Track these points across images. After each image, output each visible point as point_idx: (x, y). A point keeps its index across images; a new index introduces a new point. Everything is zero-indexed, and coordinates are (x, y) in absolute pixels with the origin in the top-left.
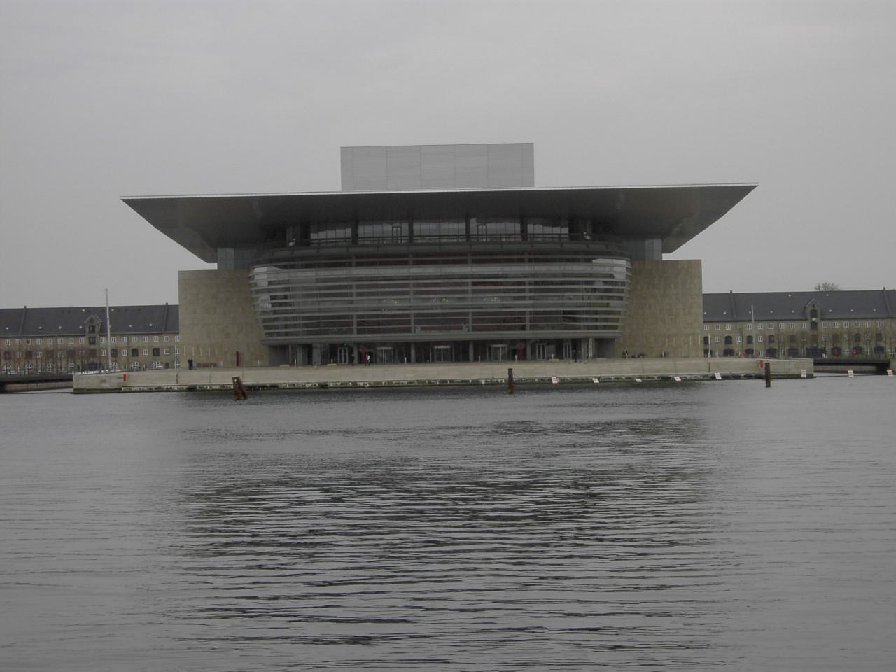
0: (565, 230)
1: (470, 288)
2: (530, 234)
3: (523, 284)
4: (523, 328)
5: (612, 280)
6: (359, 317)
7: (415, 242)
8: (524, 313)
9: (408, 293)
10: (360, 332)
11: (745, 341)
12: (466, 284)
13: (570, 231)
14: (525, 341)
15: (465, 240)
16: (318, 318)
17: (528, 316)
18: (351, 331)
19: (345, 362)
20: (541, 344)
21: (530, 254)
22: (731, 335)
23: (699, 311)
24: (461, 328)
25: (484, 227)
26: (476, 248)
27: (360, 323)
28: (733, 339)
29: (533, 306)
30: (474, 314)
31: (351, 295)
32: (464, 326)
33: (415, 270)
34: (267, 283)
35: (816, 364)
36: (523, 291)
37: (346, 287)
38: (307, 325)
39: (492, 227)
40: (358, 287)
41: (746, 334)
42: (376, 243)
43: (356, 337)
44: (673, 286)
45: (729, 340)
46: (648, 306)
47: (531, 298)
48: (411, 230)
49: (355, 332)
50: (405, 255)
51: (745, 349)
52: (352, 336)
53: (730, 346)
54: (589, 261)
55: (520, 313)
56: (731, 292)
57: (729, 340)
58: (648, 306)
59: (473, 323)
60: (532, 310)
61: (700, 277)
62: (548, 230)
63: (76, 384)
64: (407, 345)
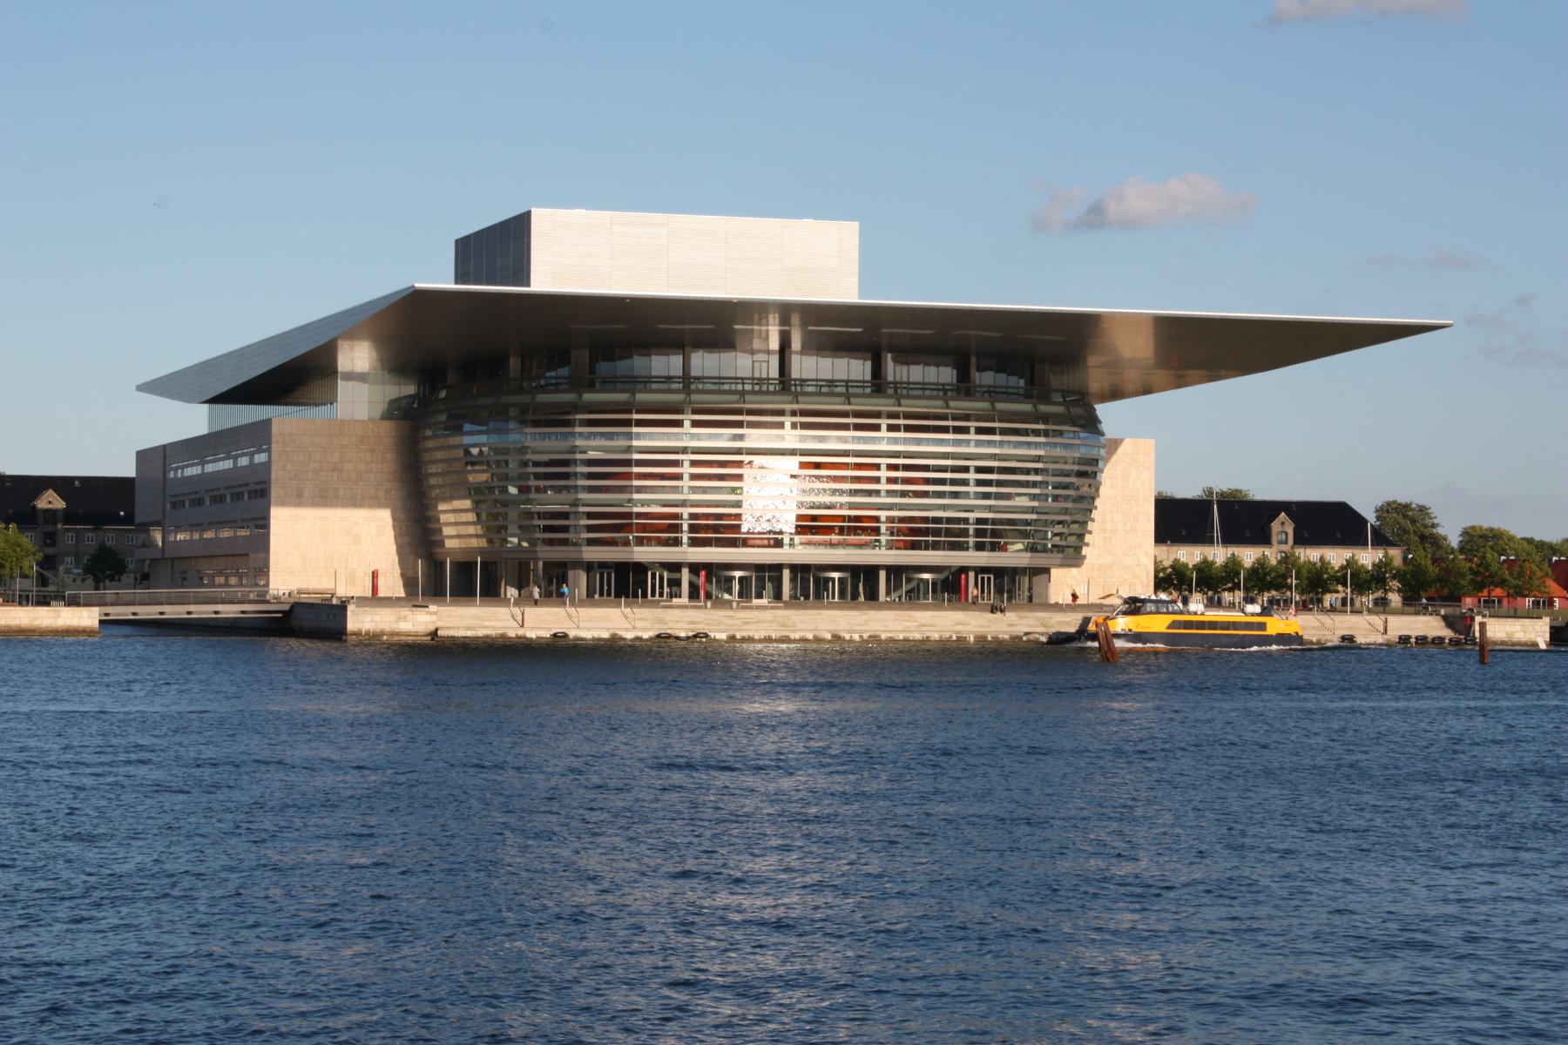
0: (1022, 383)
2: (795, 380)
6: (979, 521)
8: (966, 521)
10: (694, 542)
12: (877, 467)
13: (1026, 384)
14: (964, 570)
16: (629, 515)
18: (677, 542)
19: (609, 595)
20: (986, 576)
25: (905, 368)
27: (693, 528)
30: (890, 520)
38: (565, 529)
42: (740, 387)
48: (686, 365)
55: (959, 520)
64: (777, 568)
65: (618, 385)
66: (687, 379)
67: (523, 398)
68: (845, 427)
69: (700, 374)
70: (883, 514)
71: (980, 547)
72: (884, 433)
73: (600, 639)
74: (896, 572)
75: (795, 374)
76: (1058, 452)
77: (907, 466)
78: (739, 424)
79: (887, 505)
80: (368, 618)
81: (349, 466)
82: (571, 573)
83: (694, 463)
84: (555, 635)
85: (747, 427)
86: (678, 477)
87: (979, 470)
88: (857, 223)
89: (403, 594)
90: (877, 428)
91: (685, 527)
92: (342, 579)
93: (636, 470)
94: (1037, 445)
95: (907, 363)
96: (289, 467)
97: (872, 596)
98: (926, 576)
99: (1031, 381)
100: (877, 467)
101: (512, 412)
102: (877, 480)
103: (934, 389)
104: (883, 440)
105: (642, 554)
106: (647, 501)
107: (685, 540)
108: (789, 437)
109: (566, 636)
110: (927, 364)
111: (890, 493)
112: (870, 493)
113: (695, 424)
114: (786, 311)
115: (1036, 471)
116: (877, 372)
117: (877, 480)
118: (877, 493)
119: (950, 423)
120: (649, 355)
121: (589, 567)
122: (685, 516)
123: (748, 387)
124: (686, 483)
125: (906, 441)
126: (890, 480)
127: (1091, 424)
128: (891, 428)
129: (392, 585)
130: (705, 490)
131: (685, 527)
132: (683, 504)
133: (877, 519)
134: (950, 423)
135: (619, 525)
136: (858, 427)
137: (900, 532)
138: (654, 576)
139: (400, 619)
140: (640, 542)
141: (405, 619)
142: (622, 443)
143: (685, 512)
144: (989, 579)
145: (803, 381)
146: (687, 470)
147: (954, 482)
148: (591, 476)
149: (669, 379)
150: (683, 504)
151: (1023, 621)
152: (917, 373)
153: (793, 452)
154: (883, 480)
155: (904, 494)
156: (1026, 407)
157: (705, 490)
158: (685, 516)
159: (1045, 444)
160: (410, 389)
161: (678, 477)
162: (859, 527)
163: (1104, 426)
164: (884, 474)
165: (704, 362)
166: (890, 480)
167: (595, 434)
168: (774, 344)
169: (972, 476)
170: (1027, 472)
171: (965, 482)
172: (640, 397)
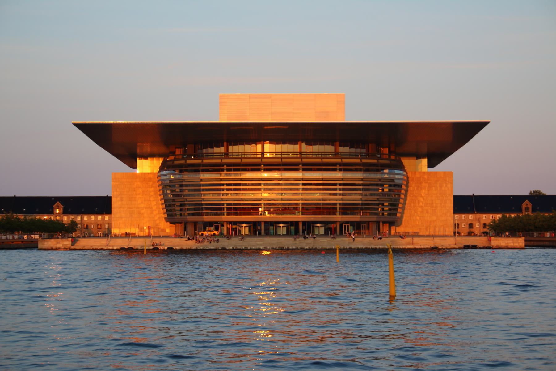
0: (364, 151)
1: (301, 187)
3: (335, 185)
4: (334, 214)
5: (394, 183)
7: (265, 156)
8: (335, 204)
9: (260, 189)
10: (229, 214)
11: (482, 225)
15: (299, 156)
16: (201, 205)
17: (338, 206)
18: (223, 214)
20: (346, 225)
21: (340, 165)
22: (472, 223)
23: (450, 205)
24: (294, 213)
25: (311, 147)
26: (305, 160)
28: (474, 225)
29: (342, 199)
30: (303, 204)
31: (223, 190)
32: (296, 211)
33: (266, 175)
34: (168, 182)
35: (526, 241)
36: (335, 189)
37: (219, 185)
38: (195, 209)
39: (316, 148)
40: (228, 185)
41: (482, 222)
42: (240, 156)
43: (226, 218)
44: (434, 188)
45: (471, 226)
46: (417, 201)
47: (340, 194)
49: (225, 214)
50: (260, 165)
51: (482, 231)
52: (223, 217)
53: (472, 230)
54: (378, 170)
56: (473, 194)
57: (471, 226)
58: (417, 201)
59: (302, 210)
60: (341, 202)
61: (452, 183)
62: (353, 150)
63: (40, 246)
64: (259, 223)
65: (209, 157)
71: (342, 214)
85: (242, 171)
91: (225, 209)
95: (311, 145)
96: (118, 190)
103: (354, 155)
112: (334, 194)
123: (243, 156)
127: (401, 167)
131: (225, 209)
139: (58, 243)
140: (207, 214)
144: (348, 226)
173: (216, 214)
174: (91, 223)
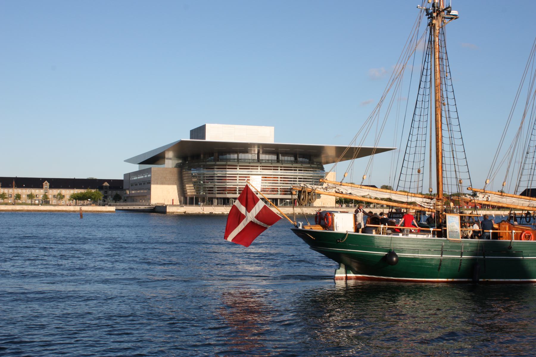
0: (308, 160)
12: (278, 178)
16: (226, 188)
25: (284, 157)
27: (239, 190)
38: (212, 191)
42: (249, 161)
48: (238, 157)
66: (238, 159)
67: (204, 163)
68: (271, 169)
69: (241, 158)
70: (279, 188)
72: (279, 171)
73: (219, 214)
74: (282, 200)
75: (261, 158)
76: (316, 175)
77: (285, 179)
78: (249, 169)
79: (280, 186)
80: (171, 209)
81: (168, 177)
82: (214, 200)
83: (239, 177)
84: (210, 213)
86: (236, 180)
87: (299, 178)
88: (273, 127)
89: (179, 204)
90: (278, 170)
91: (238, 190)
92: (166, 201)
93: (227, 178)
94: (311, 173)
95: (284, 156)
96: (155, 177)
97: (277, 205)
98: (288, 201)
99: (310, 160)
100: (278, 178)
101: (202, 166)
102: (278, 180)
104: (279, 172)
105: (229, 196)
106: (230, 185)
107: (238, 193)
108: (259, 171)
109: (212, 213)
110: (288, 156)
111: (280, 183)
112: (276, 183)
113: (240, 169)
114: (259, 145)
115: (311, 179)
116: (278, 158)
117: (278, 180)
118: (278, 183)
119: (293, 169)
120: (230, 154)
121: (218, 198)
122: (238, 188)
123: (251, 161)
124: (238, 181)
125: (284, 172)
126: (281, 181)
127: (322, 169)
128: (281, 170)
129: (177, 202)
130: (242, 182)
131: (238, 190)
132: (237, 185)
133: (278, 189)
134: (293, 169)
135: (224, 190)
136: (274, 169)
137: (283, 191)
138: (231, 200)
139: (178, 209)
140: (228, 193)
141: (179, 209)
142: (225, 173)
143: (238, 187)
145: (262, 160)
146: (238, 178)
147: (294, 181)
148: (218, 179)
149: (234, 159)
150: (237, 185)
151: (308, 210)
152: (286, 158)
153: (260, 175)
154: (279, 181)
155: (283, 183)
156: (309, 165)
157: (242, 182)
158: (238, 188)
159: (313, 173)
160: (180, 161)
161: (236, 180)
162: (274, 191)
163: (325, 169)
164: (279, 179)
165: (242, 156)
166: (281, 181)
167: (219, 171)
168: (256, 152)
169: (298, 180)
170: (309, 179)
171: (296, 181)
172: (228, 163)
173: (233, 193)
174: (67, 195)
